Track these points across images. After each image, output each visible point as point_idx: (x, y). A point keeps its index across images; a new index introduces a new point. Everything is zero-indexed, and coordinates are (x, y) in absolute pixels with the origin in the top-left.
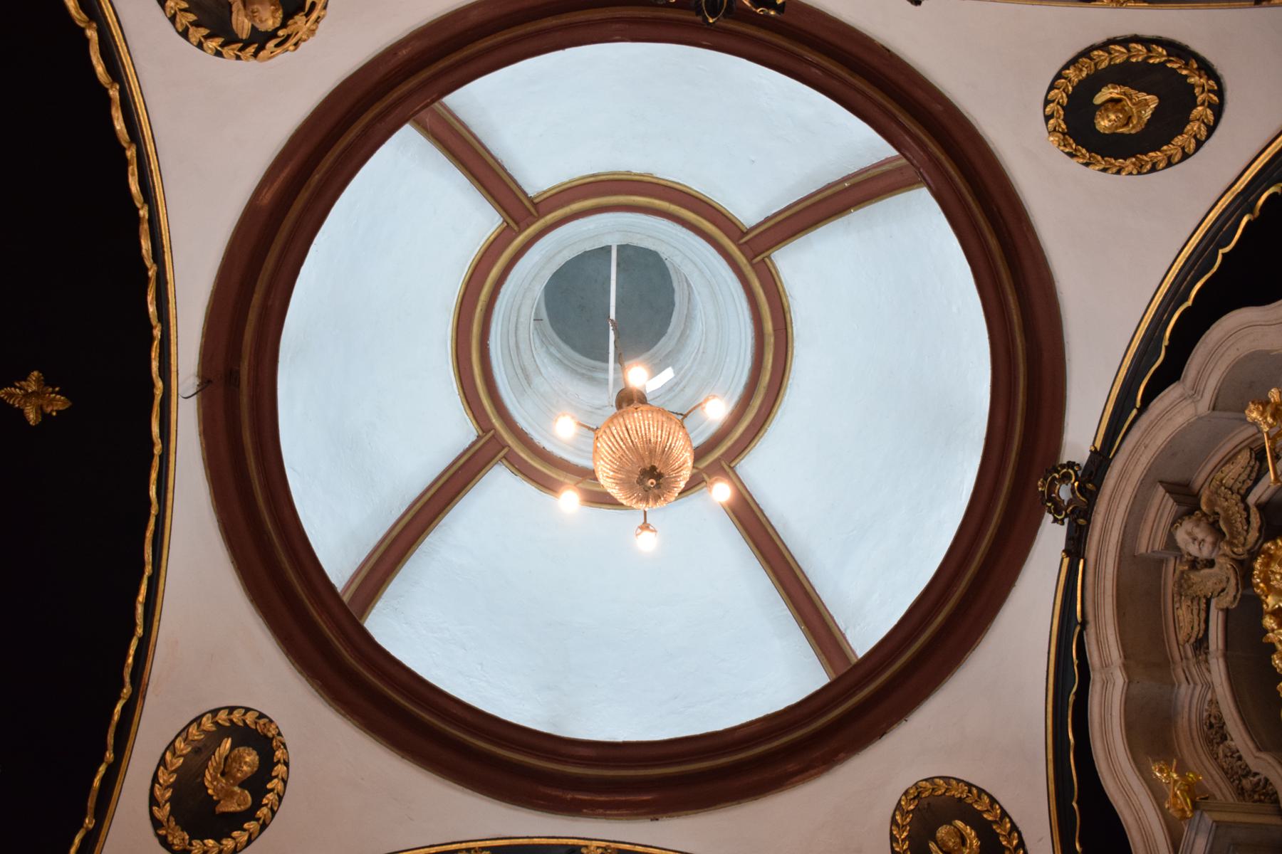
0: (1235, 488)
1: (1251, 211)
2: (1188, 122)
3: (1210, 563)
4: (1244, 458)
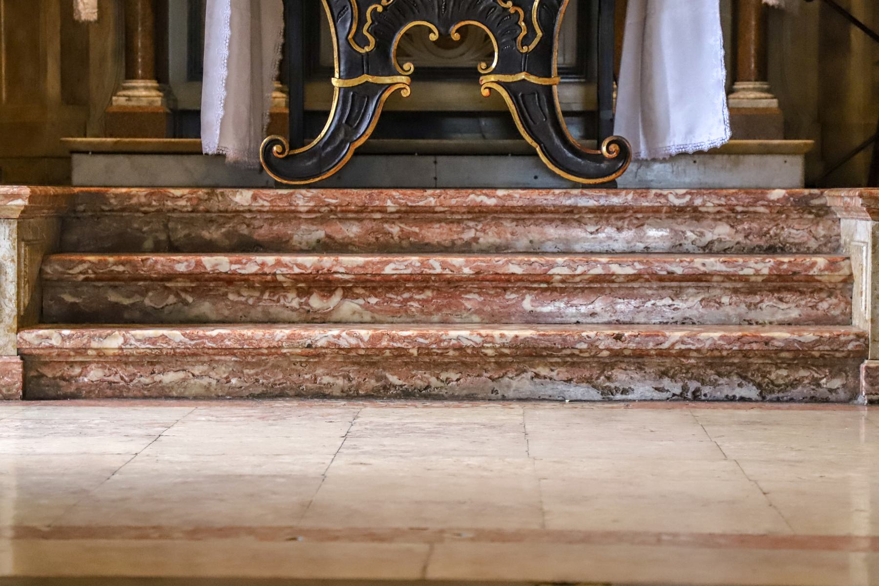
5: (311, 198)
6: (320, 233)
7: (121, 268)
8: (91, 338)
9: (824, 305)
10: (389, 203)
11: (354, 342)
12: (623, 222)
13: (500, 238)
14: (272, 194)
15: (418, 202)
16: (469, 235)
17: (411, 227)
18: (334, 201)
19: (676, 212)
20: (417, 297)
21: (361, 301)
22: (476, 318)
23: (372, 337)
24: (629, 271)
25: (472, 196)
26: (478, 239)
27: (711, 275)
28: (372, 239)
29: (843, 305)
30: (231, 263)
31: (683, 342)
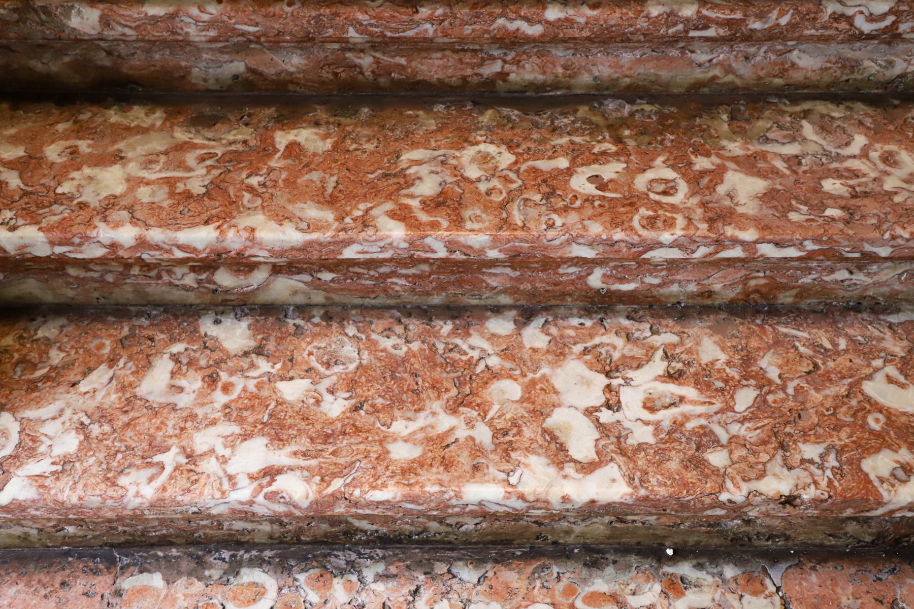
5: (210, 24)
10: (352, 33)
12: (759, 49)
13: (544, 73)
14: (136, 16)
15: (404, 31)
17: (393, 57)
18: (252, 29)
25: (501, 21)
26: (508, 74)
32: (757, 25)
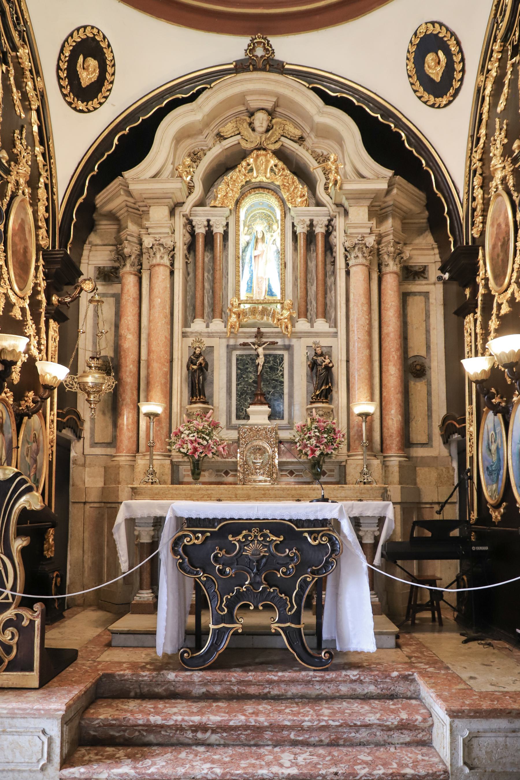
0: (285, 131)
1: (395, 127)
2: (429, 94)
3: (253, 130)
4: (298, 133)
6: (204, 690)
7: (114, 722)
8: (93, 773)
9: (420, 736)
11: (214, 776)
16: (266, 690)
19: (353, 681)
20: (244, 733)
21: (219, 735)
22: (270, 743)
23: (222, 774)
24: (337, 723)
27: (373, 725)
28: (225, 692)
29: (428, 735)
30: (162, 720)
31: (366, 776)
32: (328, 677)
